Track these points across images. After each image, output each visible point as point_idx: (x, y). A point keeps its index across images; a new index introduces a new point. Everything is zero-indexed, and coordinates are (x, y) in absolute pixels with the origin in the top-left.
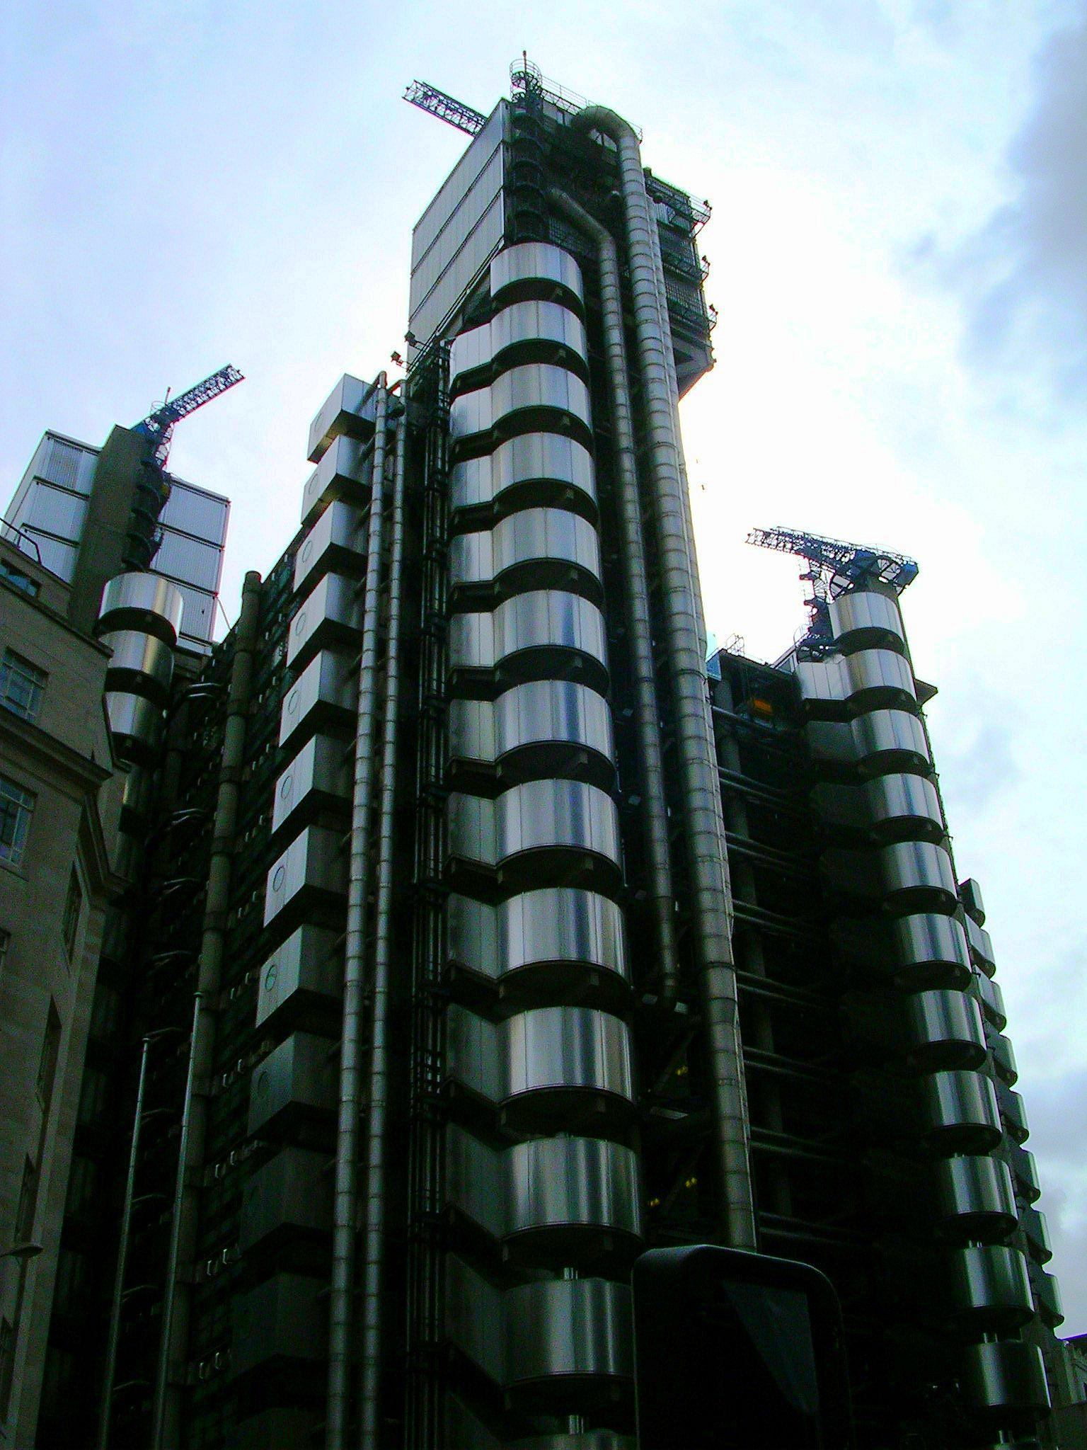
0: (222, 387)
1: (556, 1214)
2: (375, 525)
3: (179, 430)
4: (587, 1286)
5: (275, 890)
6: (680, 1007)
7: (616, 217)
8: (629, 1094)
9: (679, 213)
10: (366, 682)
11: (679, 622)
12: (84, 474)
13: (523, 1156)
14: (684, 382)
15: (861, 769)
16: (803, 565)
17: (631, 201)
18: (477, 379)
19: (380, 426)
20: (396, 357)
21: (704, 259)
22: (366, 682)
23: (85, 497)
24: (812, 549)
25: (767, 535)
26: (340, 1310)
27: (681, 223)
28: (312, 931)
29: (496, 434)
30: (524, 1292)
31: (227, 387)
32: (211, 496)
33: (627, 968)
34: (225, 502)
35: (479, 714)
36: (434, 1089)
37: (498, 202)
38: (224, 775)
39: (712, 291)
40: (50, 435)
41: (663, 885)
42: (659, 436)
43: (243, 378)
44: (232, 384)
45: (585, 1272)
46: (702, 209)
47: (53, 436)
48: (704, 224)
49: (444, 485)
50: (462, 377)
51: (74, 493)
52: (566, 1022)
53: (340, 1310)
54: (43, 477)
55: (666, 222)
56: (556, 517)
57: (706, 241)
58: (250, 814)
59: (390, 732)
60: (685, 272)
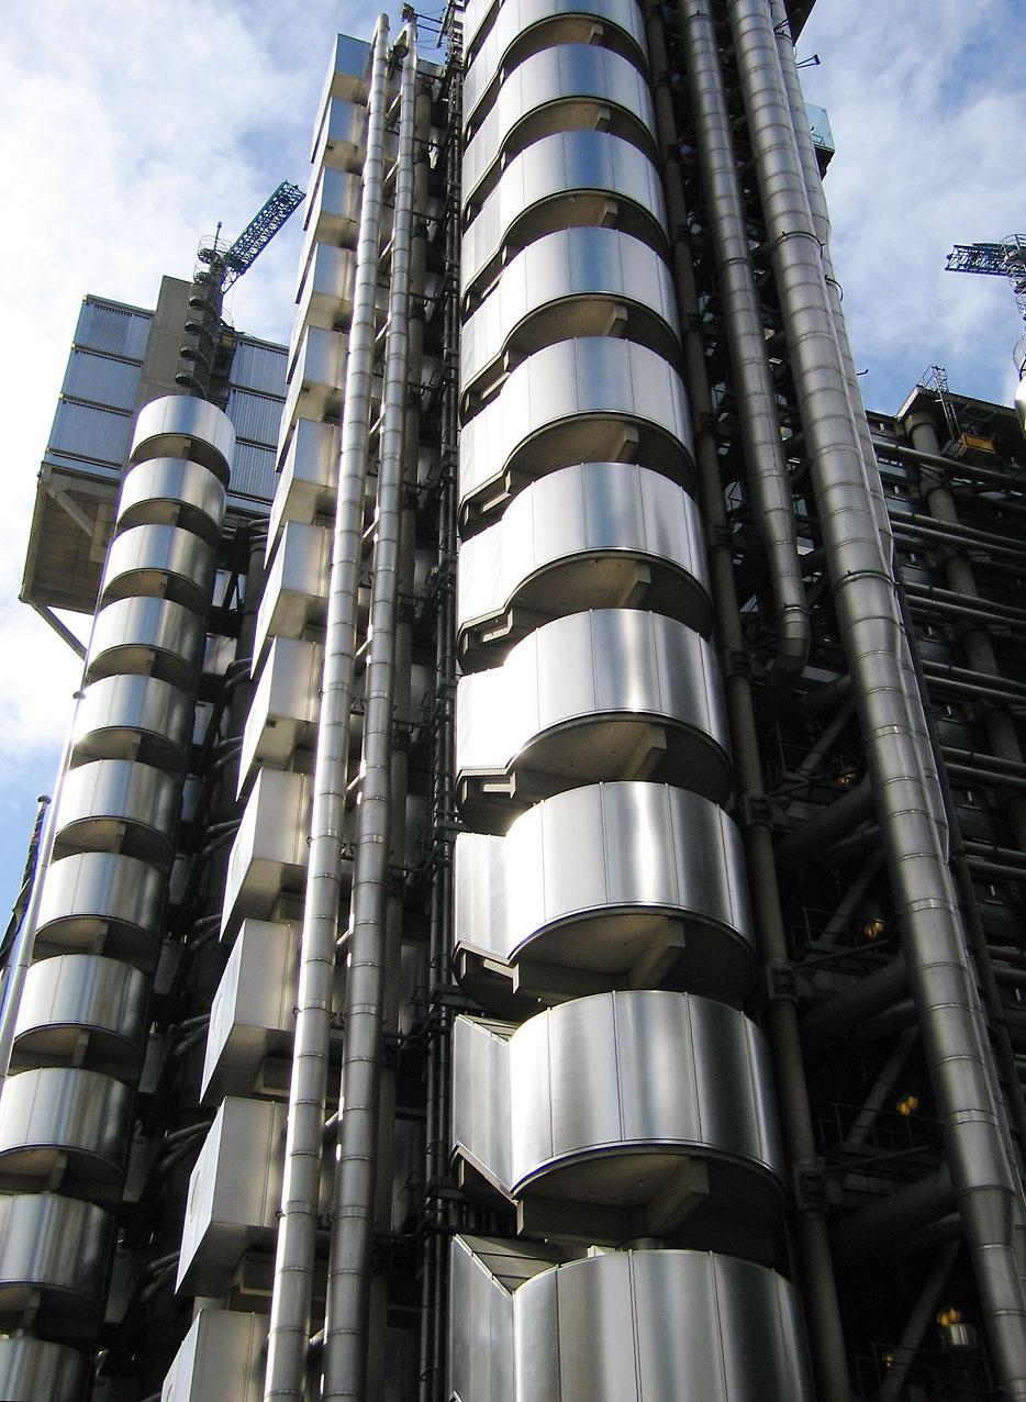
8: (710, 722)
12: (136, 339)
23: (138, 363)
33: (702, 574)
41: (773, 494)
51: (123, 359)
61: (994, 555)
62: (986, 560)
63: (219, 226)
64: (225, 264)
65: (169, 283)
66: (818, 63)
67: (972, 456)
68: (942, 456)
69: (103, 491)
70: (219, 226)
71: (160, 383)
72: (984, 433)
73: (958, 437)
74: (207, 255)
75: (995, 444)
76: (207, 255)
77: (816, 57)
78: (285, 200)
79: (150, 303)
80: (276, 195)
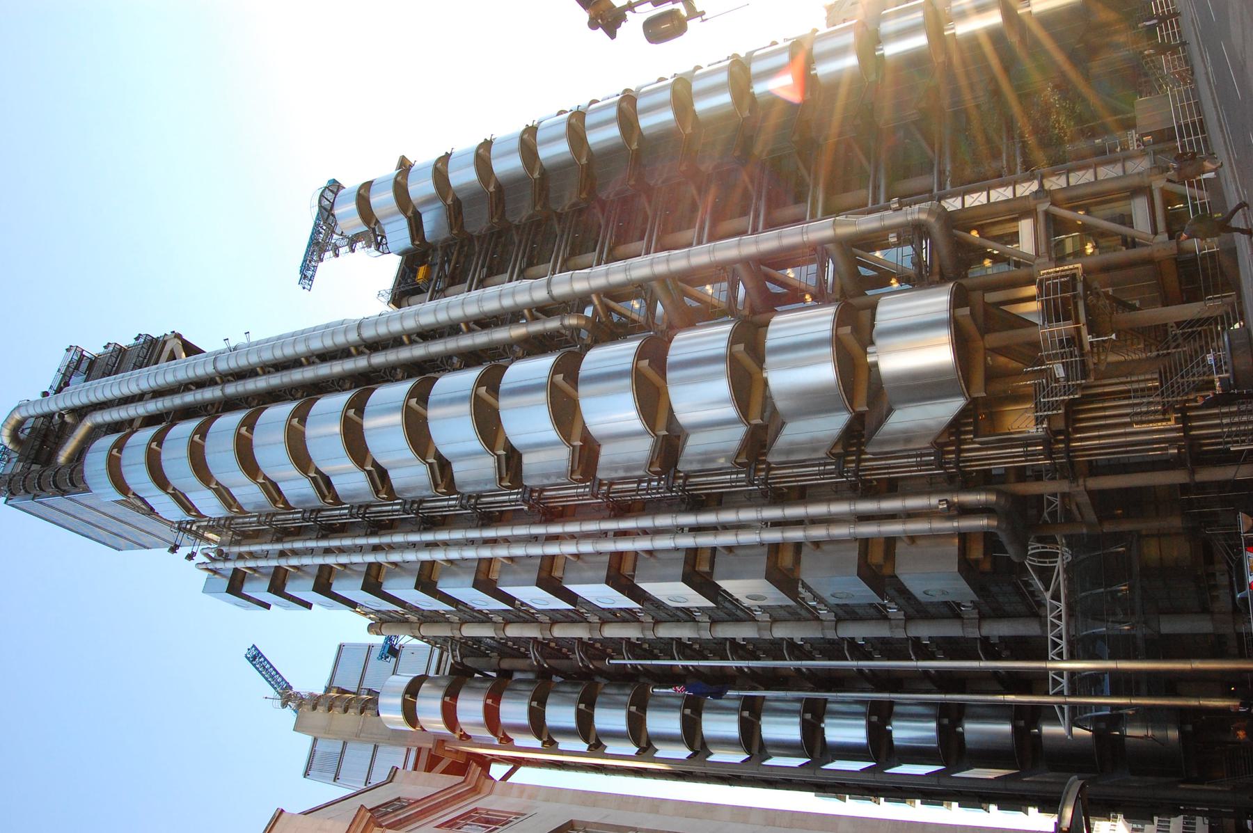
0: (262, 659)
6: (589, 312)
7: (81, 412)
9: (77, 368)
14: (190, 349)
15: (449, 201)
18: (224, 494)
20: (190, 557)
21: (105, 347)
23: (345, 744)
26: (819, 533)
27: (84, 366)
30: (780, 405)
31: (262, 656)
32: (337, 657)
34: (341, 647)
35: (398, 478)
36: (662, 479)
37: (77, 499)
39: (126, 340)
40: (306, 774)
43: (254, 646)
44: (259, 652)
46: (73, 351)
47: (306, 772)
48: (83, 350)
51: (343, 752)
52: (589, 396)
53: (819, 533)
54: (333, 775)
55: (85, 376)
56: (258, 438)
57: (94, 348)
59: (428, 537)
60: (116, 360)
61: (483, 267)
62: (485, 270)
63: (266, 698)
65: (297, 728)
66: (248, 332)
67: (428, 278)
68: (428, 292)
69: (424, 756)
70: (266, 698)
71: (360, 728)
72: (415, 272)
73: (418, 284)
74: (284, 705)
75: (421, 266)
76: (284, 705)
77: (246, 333)
78: (254, 658)
79: (307, 740)
80: (251, 662)
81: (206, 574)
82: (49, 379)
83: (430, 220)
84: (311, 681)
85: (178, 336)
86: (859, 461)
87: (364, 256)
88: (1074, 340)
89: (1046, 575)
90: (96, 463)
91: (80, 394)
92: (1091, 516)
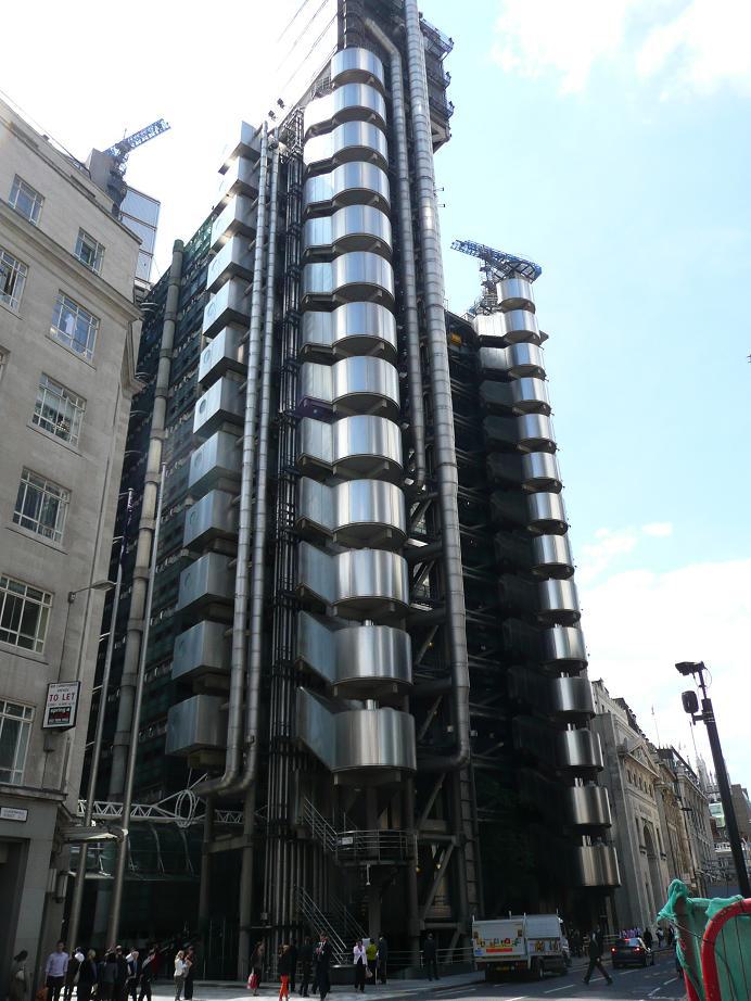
1: (363, 591)
2: (261, 210)
3: (132, 155)
4: (380, 629)
5: (201, 411)
7: (401, 42)
10: (256, 298)
11: (431, 278)
13: (345, 559)
14: (436, 145)
15: (511, 374)
16: (482, 263)
17: (410, 31)
19: (263, 152)
21: (448, 73)
22: (256, 298)
24: (488, 256)
25: (463, 244)
27: (435, 50)
28: (223, 434)
29: (334, 161)
30: (346, 632)
38: (162, 354)
39: (451, 94)
42: (423, 172)
45: (377, 622)
46: (448, 43)
49: (300, 193)
50: (312, 128)
57: (449, 63)
58: (178, 375)
64: (125, 147)
65: (95, 152)
81: (257, 128)
82: (432, 21)
83: (501, 355)
84: (136, 173)
85: (447, 139)
86: (286, 679)
87: (476, 293)
88: (365, 855)
89: (170, 806)
90: (364, 60)
91: (418, 46)
92: (217, 848)
